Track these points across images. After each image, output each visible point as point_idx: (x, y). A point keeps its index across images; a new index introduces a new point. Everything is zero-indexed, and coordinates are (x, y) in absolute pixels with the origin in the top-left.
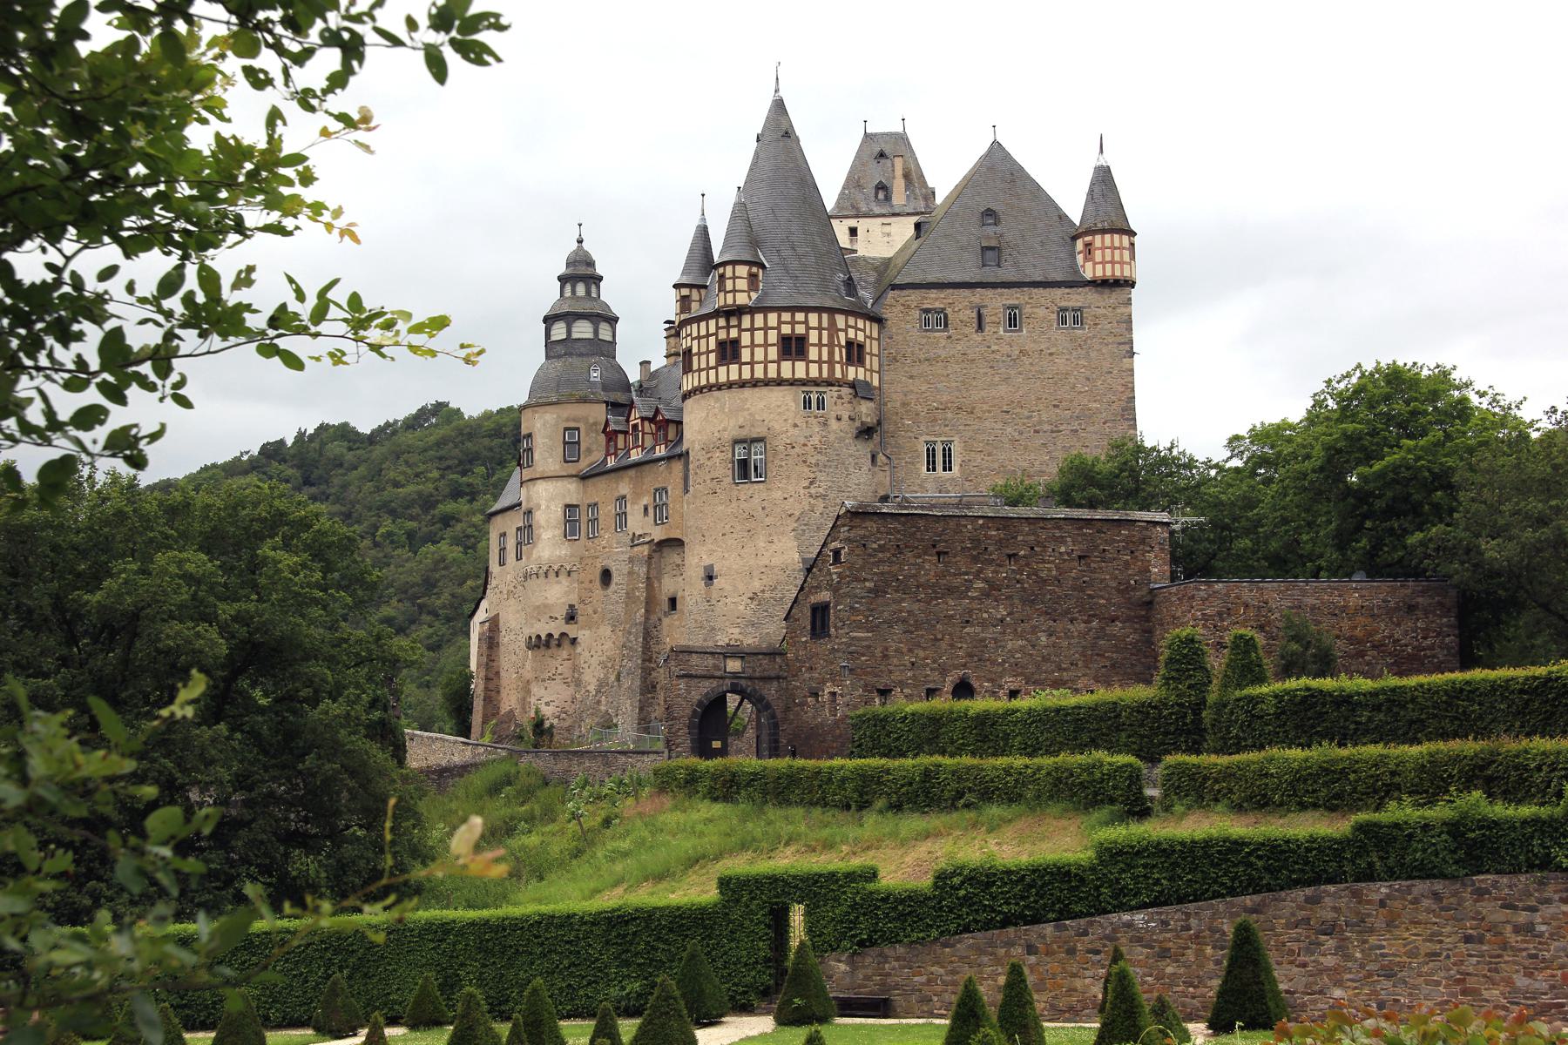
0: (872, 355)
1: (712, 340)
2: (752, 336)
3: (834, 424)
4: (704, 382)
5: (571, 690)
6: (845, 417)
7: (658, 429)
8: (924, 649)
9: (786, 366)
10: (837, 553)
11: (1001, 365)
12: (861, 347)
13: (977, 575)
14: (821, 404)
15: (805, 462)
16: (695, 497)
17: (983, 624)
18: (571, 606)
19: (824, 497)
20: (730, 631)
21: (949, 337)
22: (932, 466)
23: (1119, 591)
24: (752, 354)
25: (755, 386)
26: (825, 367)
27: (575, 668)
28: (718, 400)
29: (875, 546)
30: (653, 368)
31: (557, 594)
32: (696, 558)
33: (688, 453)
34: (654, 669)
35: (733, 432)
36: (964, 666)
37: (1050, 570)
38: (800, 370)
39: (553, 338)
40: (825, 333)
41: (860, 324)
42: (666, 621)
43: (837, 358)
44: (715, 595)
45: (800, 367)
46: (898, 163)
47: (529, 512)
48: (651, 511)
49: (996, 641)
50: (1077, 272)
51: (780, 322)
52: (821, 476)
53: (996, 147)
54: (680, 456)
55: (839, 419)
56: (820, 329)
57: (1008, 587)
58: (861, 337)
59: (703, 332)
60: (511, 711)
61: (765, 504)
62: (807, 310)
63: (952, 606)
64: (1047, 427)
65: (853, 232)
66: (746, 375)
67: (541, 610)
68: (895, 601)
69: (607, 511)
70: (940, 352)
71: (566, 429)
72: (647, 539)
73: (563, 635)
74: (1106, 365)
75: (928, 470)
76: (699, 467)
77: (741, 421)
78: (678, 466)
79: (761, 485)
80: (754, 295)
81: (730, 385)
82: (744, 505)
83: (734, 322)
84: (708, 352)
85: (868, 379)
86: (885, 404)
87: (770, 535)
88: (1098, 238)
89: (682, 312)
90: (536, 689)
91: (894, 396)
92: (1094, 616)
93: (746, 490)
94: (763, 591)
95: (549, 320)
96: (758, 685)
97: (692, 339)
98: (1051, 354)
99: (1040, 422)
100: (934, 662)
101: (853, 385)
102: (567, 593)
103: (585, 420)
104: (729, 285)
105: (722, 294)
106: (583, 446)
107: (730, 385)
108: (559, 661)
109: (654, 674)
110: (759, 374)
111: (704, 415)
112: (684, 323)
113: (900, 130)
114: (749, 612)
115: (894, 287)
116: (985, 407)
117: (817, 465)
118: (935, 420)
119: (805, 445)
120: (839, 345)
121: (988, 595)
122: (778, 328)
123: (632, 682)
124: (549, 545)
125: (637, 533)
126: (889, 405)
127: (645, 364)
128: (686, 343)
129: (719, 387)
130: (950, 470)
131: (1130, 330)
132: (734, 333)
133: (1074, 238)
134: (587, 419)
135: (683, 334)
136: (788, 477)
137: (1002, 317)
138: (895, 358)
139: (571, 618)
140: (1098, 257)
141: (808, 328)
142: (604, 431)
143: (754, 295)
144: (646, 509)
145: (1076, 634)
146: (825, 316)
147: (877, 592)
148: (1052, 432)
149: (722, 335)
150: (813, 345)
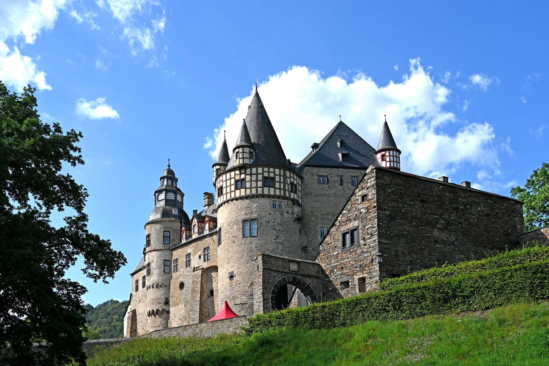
0: (299, 191)
3: (286, 215)
4: (228, 198)
6: (290, 212)
8: (416, 254)
14: (280, 206)
15: (274, 229)
19: (282, 243)
21: (329, 187)
24: (251, 184)
25: (252, 197)
26: (282, 191)
29: (389, 191)
34: (204, 318)
41: (295, 177)
43: (287, 188)
45: (272, 190)
49: (451, 254)
51: (263, 172)
52: (281, 235)
54: (216, 232)
55: (288, 213)
56: (280, 175)
57: (455, 225)
58: (295, 182)
69: (182, 261)
72: (200, 268)
73: (164, 310)
78: (215, 237)
80: (252, 161)
83: (243, 171)
84: (231, 185)
85: (298, 200)
86: (304, 211)
91: (308, 209)
103: (172, 228)
106: (171, 238)
117: (279, 230)
118: (324, 219)
119: (274, 222)
120: (287, 183)
121: (446, 228)
122: (262, 174)
125: (196, 267)
126: (306, 212)
127: (195, 211)
129: (237, 199)
132: (243, 176)
134: (173, 228)
136: (267, 235)
138: (307, 194)
140: (388, 159)
141: (275, 175)
144: (200, 257)
146: (282, 171)
147: (392, 217)
149: (237, 177)
150: (277, 182)
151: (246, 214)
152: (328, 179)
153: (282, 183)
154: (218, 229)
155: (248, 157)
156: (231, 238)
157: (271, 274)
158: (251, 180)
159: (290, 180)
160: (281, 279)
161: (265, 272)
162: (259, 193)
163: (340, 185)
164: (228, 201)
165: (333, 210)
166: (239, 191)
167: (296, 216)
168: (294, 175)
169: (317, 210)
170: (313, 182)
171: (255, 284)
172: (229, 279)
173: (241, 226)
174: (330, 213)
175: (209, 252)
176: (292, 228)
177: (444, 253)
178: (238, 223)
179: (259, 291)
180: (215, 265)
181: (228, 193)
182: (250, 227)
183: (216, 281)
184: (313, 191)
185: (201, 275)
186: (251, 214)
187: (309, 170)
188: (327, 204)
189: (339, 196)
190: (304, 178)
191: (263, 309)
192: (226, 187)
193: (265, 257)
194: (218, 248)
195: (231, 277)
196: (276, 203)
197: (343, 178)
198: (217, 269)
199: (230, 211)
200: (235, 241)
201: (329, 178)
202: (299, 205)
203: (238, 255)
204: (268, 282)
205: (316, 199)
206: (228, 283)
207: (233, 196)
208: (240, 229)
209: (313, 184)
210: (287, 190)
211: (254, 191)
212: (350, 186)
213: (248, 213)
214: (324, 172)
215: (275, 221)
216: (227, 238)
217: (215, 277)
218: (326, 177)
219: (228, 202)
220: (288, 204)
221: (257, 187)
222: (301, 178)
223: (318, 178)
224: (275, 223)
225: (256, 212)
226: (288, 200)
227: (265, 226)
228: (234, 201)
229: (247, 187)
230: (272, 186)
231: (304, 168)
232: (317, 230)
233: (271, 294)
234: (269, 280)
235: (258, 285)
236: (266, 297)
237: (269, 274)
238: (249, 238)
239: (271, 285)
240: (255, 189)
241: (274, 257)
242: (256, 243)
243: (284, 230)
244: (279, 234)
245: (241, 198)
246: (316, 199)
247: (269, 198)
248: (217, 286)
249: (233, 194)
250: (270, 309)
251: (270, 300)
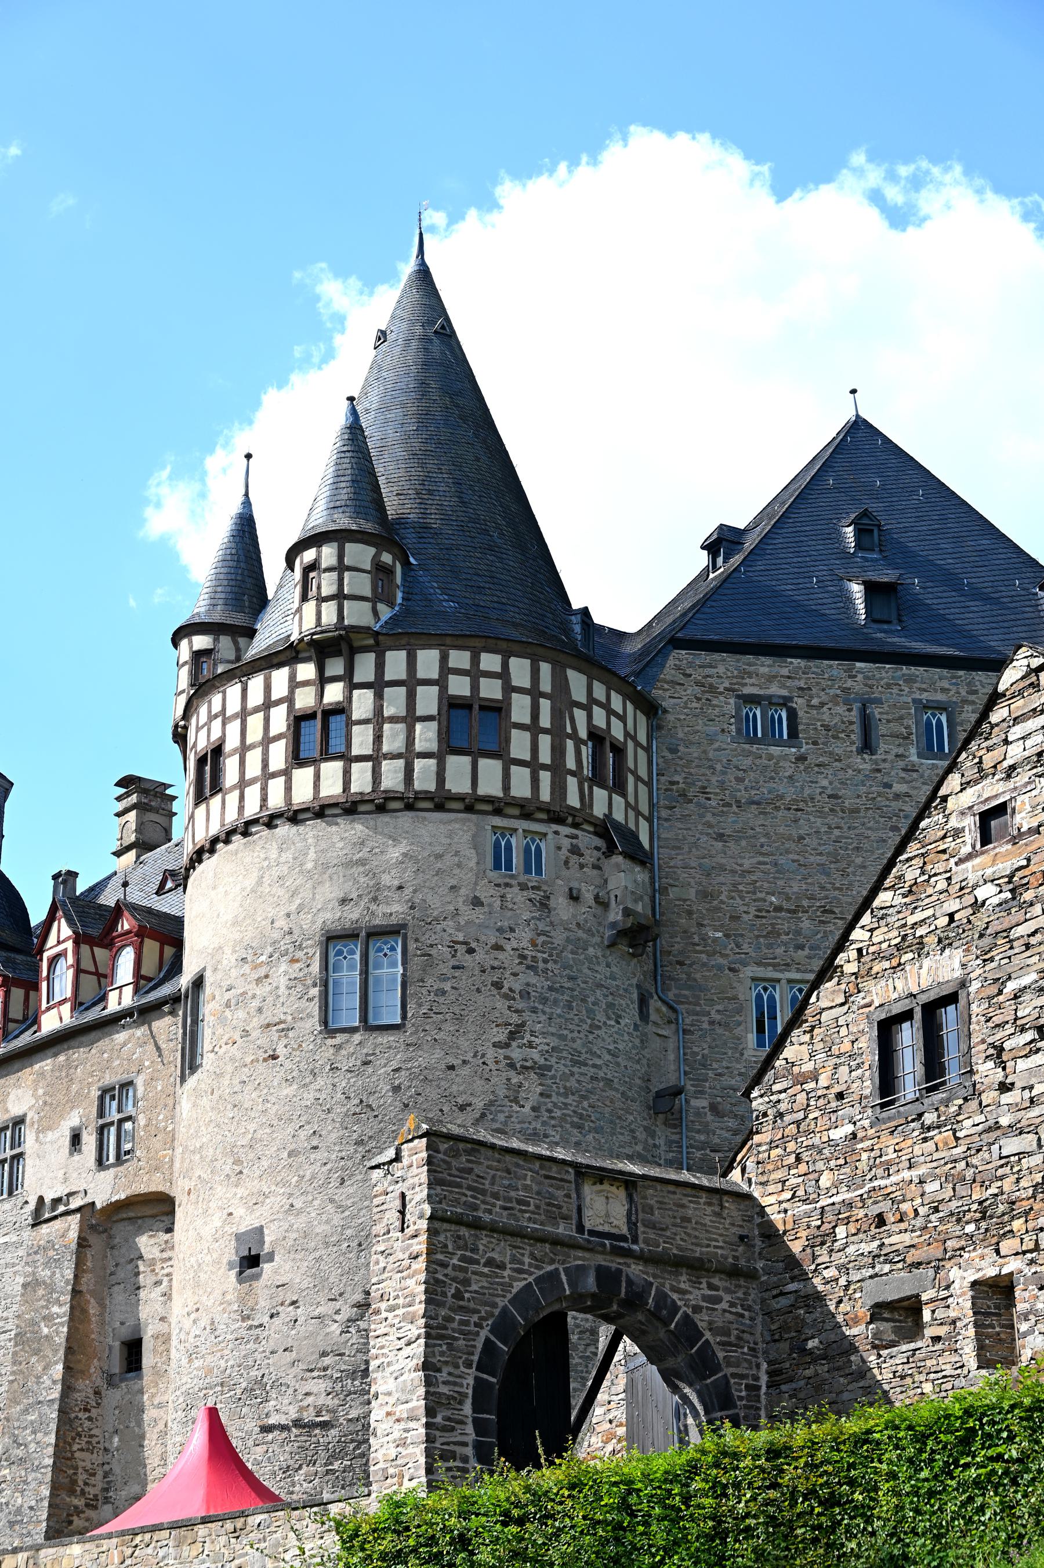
0: (638, 778)
4: (252, 808)
6: (588, 895)
9: (458, 766)
14: (533, 860)
15: (498, 985)
21: (801, 758)
24: (378, 738)
25: (381, 809)
26: (545, 777)
34: (78, 1512)
40: (545, 705)
41: (617, 702)
43: (571, 764)
45: (490, 769)
51: (445, 670)
54: (175, 999)
55: (574, 897)
56: (535, 693)
58: (617, 731)
72: (76, 1203)
80: (385, 612)
83: (336, 667)
84: (267, 740)
85: (632, 825)
86: (664, 890)
117: (525, 995)
118: (774, 933)
119: (498, 947)
120: (574, 737)
122: (441, 683)
126: (673, 893)
129: (295, 816)
132: (334, 693)
136: (459, 1019)
138: (683, 794)
141: (509, 689)
144: (76, 1139)
146: (545, 668)
149: (305, 700)
151: (344, 901)
152: (792, 715)
153: (545, 731)
154: (184, 981)
156: (255, 1034)
157: (474, 1250)
158: (378, 710)
159: (590, 717)
160: (531, 1279)
161: (442, 1238)
162: (417, 785)
163: (861, 751)
164: (246, 829)
165: (823, 888)
166: (309, 772)
167: (620, 917)
168: (613, 693)
169: (734, 885)
170: (713, 729)
171: (383, 1306)
172: (233, 1273)
173: (316, 967)
174: (805, 903)
175: (130, 1110)
176: (600, 986)
178: (300, 947)
179: (408, 1351)
180: (161, 1188)
181: (253, 781)
182: (365, 973)
183: (158, 1283)
184: (714, 779)
185: (74, 1246)
186: (375, 899)
187: (691, 664)
188: (788, 852)
189: (857, 811)
190: (665, 711)
191: (422, 1460)
192: (244, 749)
193: (443, 1147)
194: (179, 1091)
195: (251, 1262)
196: (513, 841)
198: (172, 1213)
199: (260, 882)
200: (281, 1051)
201: (800, 714)
202: (638, 856)
203: (290, 1130)
204: (458, 1296)
205: (729, 824)
206: (228, 1297)
207: (276, 800)
208: (309, 982)
209: (711, 741)
210: (573, 774)
211: (392, 776)
213: (354, 896)
215: (502, 942)
216: (236, 1036)
217: (152, 1262)
218: (784, 705)
219: (246, 834)
220: (575, 850)
221: (409, 755)
222: (650, 708)
223: (738, 709)
224: (501, 956)
225: (400, 888)
226: (576, 825)
227: (445, 969)
228: (284, 830)
229: (355, 751)
230: (493, 747)
231: (666, 657)
232: (735, 998)
233: (472, 1371)
234: (466, 1282)
235: (400, 1312)
236: (444, 1389)
237: (465, 1248)
238: (357, 1037)
239: (475, 1318)
240: (401, 763)
241: (493, 1147)
242: (394, 1064)
243: (554, 995)
244: (527, 1016)
245: (321, 811)
246: (729, 824)
247: (473, 817)
248: (161, 1311)
249: (276, 786)
250: (465, 1459)
251: (468, 1408)
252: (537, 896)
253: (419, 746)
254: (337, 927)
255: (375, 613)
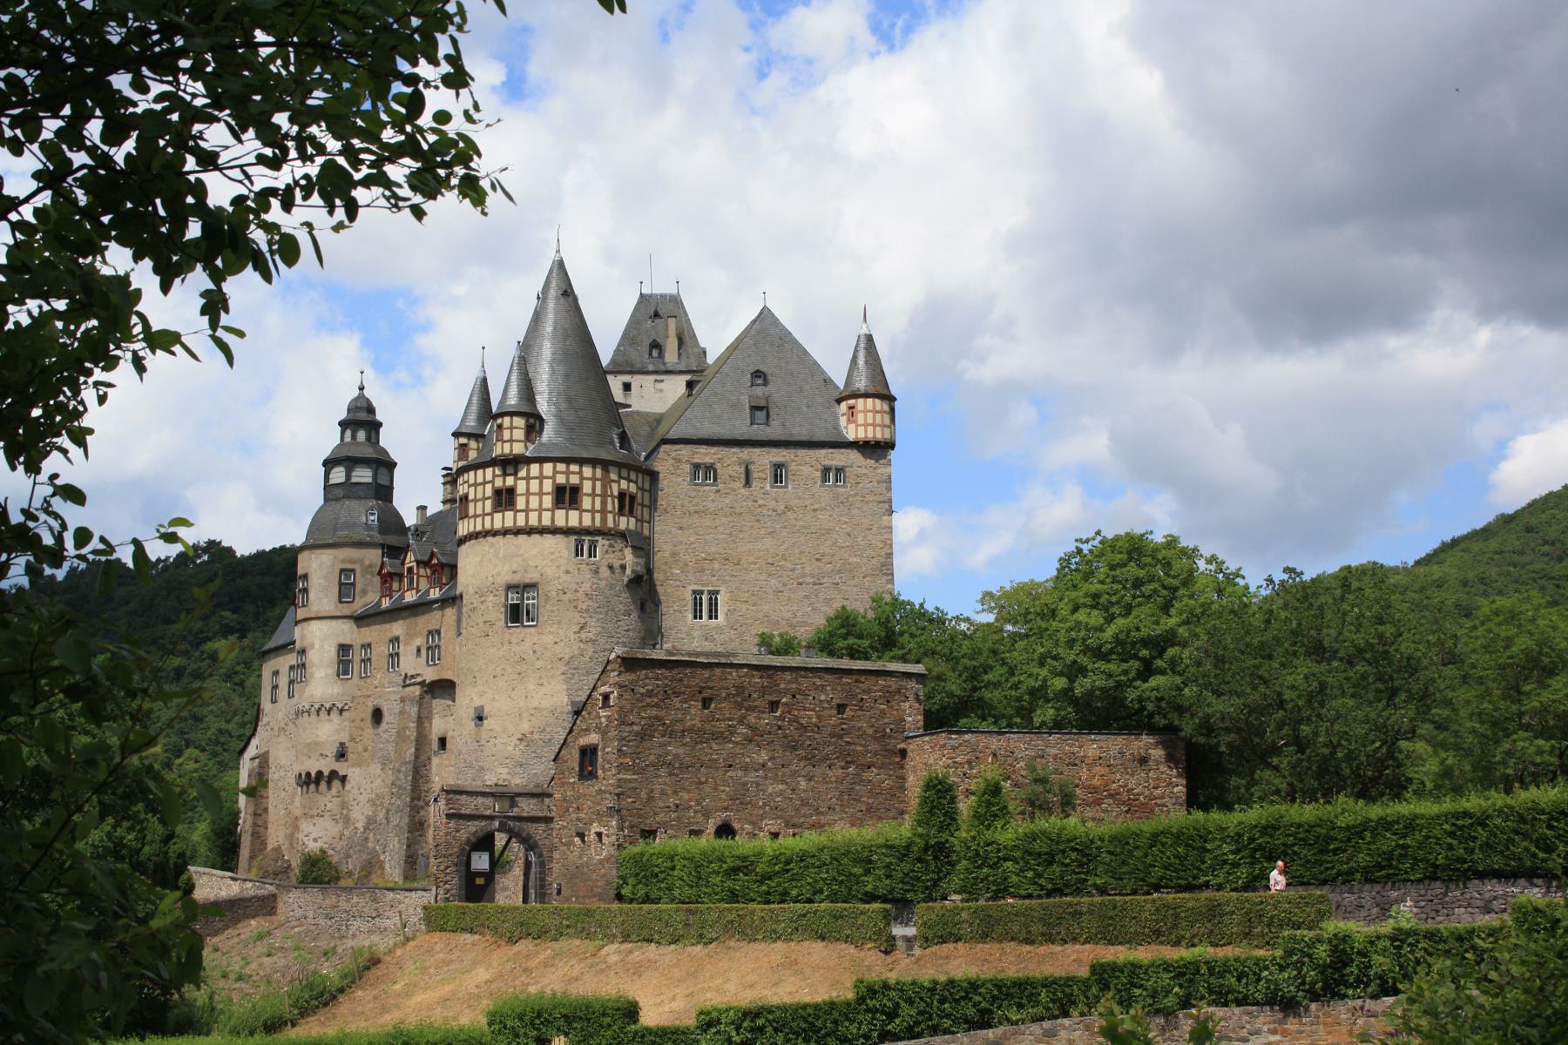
1: (489, 487)
2: (528, 484)
3: (605, 572)
4: (479, 528)
5: (340, 827)
7: (433, 573)
8: (688, 791)
9: (560, 514)
10: (606, 697)
11: (766, 518)
12: (633, 498)
13: (741, 720)
15: (576, 607)
16: (467, 639)
17: (746, 768)
18: (342, 744)
19: (593, 641)
20: (499, 771)
21: (718, 491)
22: (697, 614)
23: (875, 739)
24: (528, 502)
26: (598, 516)
27: (344, 805)
28: (492, 545)
30: (429, 513)
31: (328, 731)
32: (468, 698)
33: (461, 596)
35: (506, 577)
36: (726, 809)
37: (810, 718)
38: (574, 519)
39: (331, 482)
41: (633, 476)
42: (435, 761)
43: (610, 508)
44: (484, 735)
46: (672, 323)
47: (303, 652)
48: (424, 652)
49: (758, 785)
50: (840, 433)
51: (555, 472)
53: (765, 308)
56: (594, 479)
57: (770, 733)
59: (480, 480)
60: (279, 847)
61: (537, 647)
62: (582, 462)
63: (718, 751)
64: (809, 580)
65: (627, 387)
66: (521, 522)
67: (313, 747)
68: (661, 745)
69: (380, 651)
70: (709, 505)
71: (342, 571)
72: (419, 679)
74: (866, 522)
75: (695, 618)
76: (474, 610)
77: (514, 567)
78: (450, 612)
79: (532, 630)
81: (505, 532)
82: (516, 648)
83: (510, 470)
84: (484, 499)
87: (540, 678)
88: (861, 401)
89: (460, 459)
90: (306, 826)
92: (851, 762)
93: (517, 633)
94: (532, 733)
95: (329, 464)
96: (524, 825)
97: (469, 486)
98: (815, 510)
99: (803, 576)
100: (698, 804)
101: (623, 535)
102: (338, 732)
103: (360, 562)
104: (506, 435)
105: (499, 444)
106: (359, 587)
107: (505, 532)
108: (328, 799)
109: (422, 813)
110: (533, 521)
111: (478, 559)
112: (462, 471)
113: (674, 292)
114: (518, 753)
115: (665, 441)
116: (751, 559)
117: (587, 611)
118: (703, 570)
119: (576, 591)
120: (612, 496)
122: (553, 478)
123: (401, 820)
124: (322, 683)
125: (409, 674)
127: (423, 508)
128: (462, 490)
129: (495, 533)
130: (716, 618)
131: (889, 489)
132: (510, 481)
133: (839, 401)
135: (460, 480)
137: (769, 473)
139: (341, 755)
141: (582, 479)
142: (379, 573)
143: (531, 447)
144: (419, 650)
145: (833, 779)
147: (643, 736)
148: (815, 584)
149: (499, 483)
155: (522, 438)
177: (744, 784)
197: (752, 467)
205: (684, 522)
212: (768, 487)
214: (706, 454)
221: (540, 510)
227: (554, 601)
228: (490, 539)
252: (593, 567)
253: (544, 506)
254: (512, 583)
255: (526, 448)
